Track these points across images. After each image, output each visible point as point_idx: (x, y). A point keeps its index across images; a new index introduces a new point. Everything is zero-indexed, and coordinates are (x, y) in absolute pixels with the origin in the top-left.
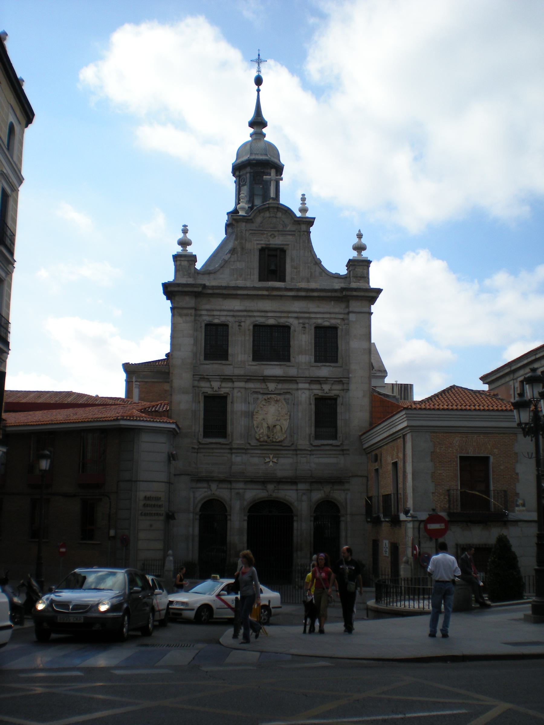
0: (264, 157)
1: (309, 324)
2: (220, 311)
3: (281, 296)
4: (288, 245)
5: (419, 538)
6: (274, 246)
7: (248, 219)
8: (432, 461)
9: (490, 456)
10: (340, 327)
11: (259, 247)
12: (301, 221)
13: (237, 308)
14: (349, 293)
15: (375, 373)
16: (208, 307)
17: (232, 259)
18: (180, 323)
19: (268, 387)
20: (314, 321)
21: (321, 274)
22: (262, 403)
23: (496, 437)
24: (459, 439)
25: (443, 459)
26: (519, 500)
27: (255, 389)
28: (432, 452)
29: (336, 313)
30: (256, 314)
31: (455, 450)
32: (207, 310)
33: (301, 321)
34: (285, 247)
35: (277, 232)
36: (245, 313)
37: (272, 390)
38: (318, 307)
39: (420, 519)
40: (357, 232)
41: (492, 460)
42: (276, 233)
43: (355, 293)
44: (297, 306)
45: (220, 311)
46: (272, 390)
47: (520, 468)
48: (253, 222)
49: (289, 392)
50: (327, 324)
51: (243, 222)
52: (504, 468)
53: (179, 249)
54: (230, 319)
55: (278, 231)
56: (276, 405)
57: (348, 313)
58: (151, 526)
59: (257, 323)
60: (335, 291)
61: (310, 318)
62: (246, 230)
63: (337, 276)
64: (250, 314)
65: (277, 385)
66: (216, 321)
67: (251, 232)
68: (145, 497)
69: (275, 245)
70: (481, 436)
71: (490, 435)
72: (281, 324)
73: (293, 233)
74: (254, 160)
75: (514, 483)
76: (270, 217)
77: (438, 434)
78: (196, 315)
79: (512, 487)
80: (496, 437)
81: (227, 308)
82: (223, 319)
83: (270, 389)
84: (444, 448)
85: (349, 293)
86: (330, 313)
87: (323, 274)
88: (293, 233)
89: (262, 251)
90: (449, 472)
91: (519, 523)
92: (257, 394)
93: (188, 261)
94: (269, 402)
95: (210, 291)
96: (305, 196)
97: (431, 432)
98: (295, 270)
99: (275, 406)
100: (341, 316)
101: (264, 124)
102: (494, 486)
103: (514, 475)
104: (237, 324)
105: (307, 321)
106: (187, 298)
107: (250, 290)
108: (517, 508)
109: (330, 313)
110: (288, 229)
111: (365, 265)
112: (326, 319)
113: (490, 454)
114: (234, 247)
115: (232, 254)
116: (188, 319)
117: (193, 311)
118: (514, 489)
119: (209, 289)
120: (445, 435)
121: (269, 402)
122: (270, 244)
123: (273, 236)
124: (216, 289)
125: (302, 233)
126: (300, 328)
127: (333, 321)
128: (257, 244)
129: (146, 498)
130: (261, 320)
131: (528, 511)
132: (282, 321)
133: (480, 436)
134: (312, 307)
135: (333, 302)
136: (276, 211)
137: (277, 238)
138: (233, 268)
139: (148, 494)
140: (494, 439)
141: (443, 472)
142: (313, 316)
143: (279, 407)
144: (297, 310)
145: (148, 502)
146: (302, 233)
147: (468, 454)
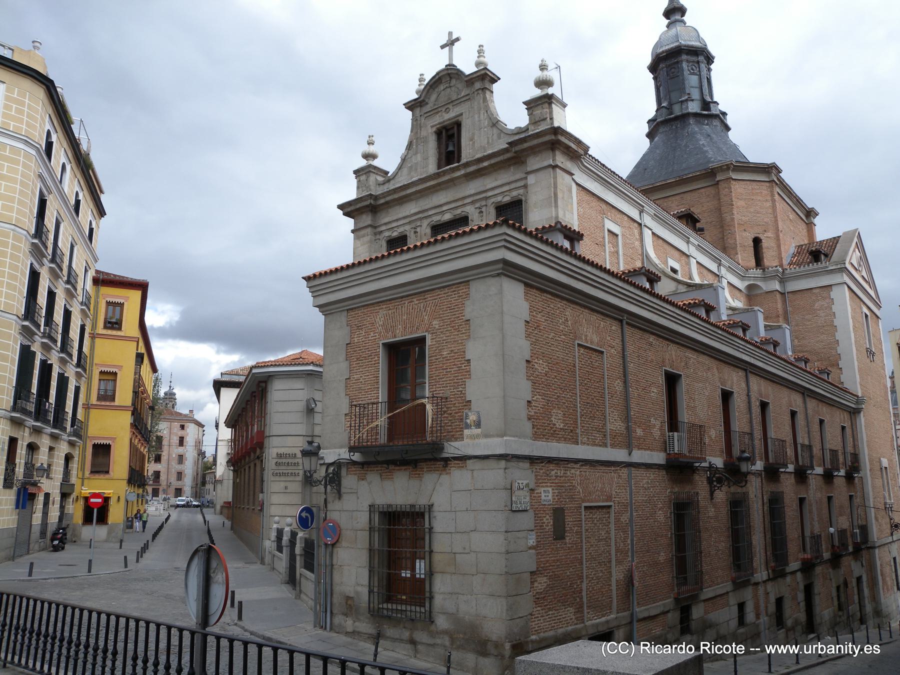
0: (677, 44)
1: (486, 205)
2: (397, 220)
3: (452, 180)
4: (462, 114)
5: (326, 493)
6: (448, 122)
7: (421, 102)
8: (347, 360)
9: (426, 334)
10: (523, 199)
11: (434, 129)
13: (413, 211)
14: (518, 148)
15: (827, 267)
16: (386, 220)
17: (409, 156)
18: (358, 247)
20: (493, 200)
21: (499, 138)
23: (435, 297)
24: (385, 312)
25: (361, 354)
26: (469, 414)
28: (347, 344)
29: (516, 181)
30: (430, 213)
31: (377, 334)
32: (386, 224)
33: (477, 205)
34: (460, 118)
35: (451, 104)
36: (421, 215)
38: (496, 180)
39: (326, 462)
40: (540, 62)
41: (428, 342)
42: (450, 106)
43: (526, 145)
44: (473, 187)
45: (397, 220)
47: (473, 350)
48: (427, 104)
50: (507, 199)
51: (417, 107)
52: (448, 354)
53: (363, 163)
54: (407, 228)
55: (452, 102)
57: (526, 178)
58: (286, 488)
60: (506, 151)
61: (486, 198)
62: (421, 116)
63: (520, 131)
64: (426, 214)
66: (395, 234)
67: (426, 115)
68: (277, 454)
69: (449, 120)
70: (415, 300)
71: (428, 296)
72: (458, 217)
73: (467, 98)
74: (663, 52)
75: (464, 380)
76: (444, 90)
77: (357, 312)
78: (375, 234)
79: (460, 389)
80: (435, 297)
81: (404, 214)
82: (401, 229)
84: (364, 334)
85: (518, 148)
86: (509, 183)
87: (502, 135)
88: (467, 98)
89: (439, 133)
90: (368, 375)
91: (468, 462)
93: (365, 173)
95: (382, 201)
96: (484, 48)
97: (348, 310)
98: (471, 143)
100: (522, 183)
101: (682, 11)
102: (431, 392)
103: (463, 366)
104: (413, 231)
105: (484, 203)
106: (364, 216)
107: (418, 184)
108: (467, 432)
109: (509, 183)
110: (463, 94)
111: (544, 103)
112: (506, 194)
113: (426, 332)
115: (409, 150)
116: (367, 239)
117: (369, 230)
118: (463, 392)
119: (381, 198)
120: (365, 310)
122: (444, 122)
123: (448, 110)
124: (388, 196)
125: (476, 93)
126: (477, 214)
127: (515, 193)
128: (432, 127)
129: (280, 456)
130: (436, 218)
131: (487, 436)
132: (459, 211)
133: (412, 302)
134: (488, 182)
135: (512, 167)
136: (448, 79)
137: (451, 111)
138: (410, 165)
139: (282, 451)
140: (434, 301)
141: (361, 377)
142: (490, 194)
144: (473, 192)
145: (284, 461)
146: (476, 93)
147: (395, 337)
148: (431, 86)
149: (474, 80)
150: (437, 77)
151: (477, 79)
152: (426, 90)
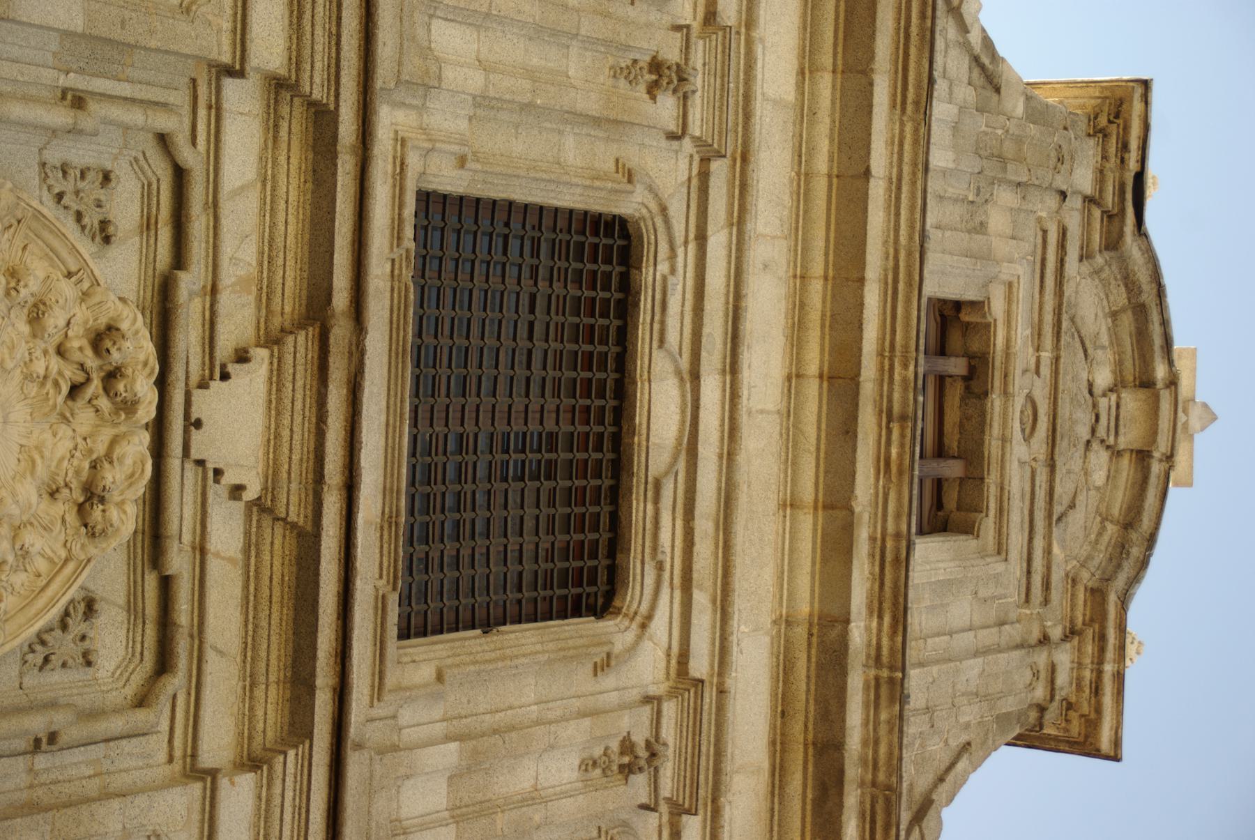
12: (1102, 638)
19: (225, 376)
22: (67, 289)
27: (214, 206)
37: (198, 424)
46: (198, 424)
49: (164, 664)
56: (29, 491)
59: (663, 268)
65: (237, 491)
83: (204, 403)
92: (148, 225)
94: (75, 390)
99: (29, 457)
114: (1002, 91)
121: (75, 390)
136: (1123, 442)
143: (17, 530)
148: (1140, 311)
149: (1089, 649)
150: (1160, 372)
151: (1087, 674)
152: (1143, 276)
